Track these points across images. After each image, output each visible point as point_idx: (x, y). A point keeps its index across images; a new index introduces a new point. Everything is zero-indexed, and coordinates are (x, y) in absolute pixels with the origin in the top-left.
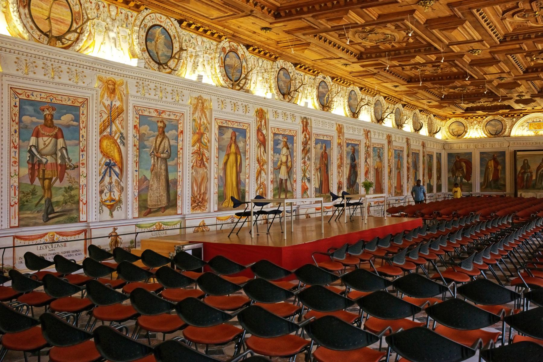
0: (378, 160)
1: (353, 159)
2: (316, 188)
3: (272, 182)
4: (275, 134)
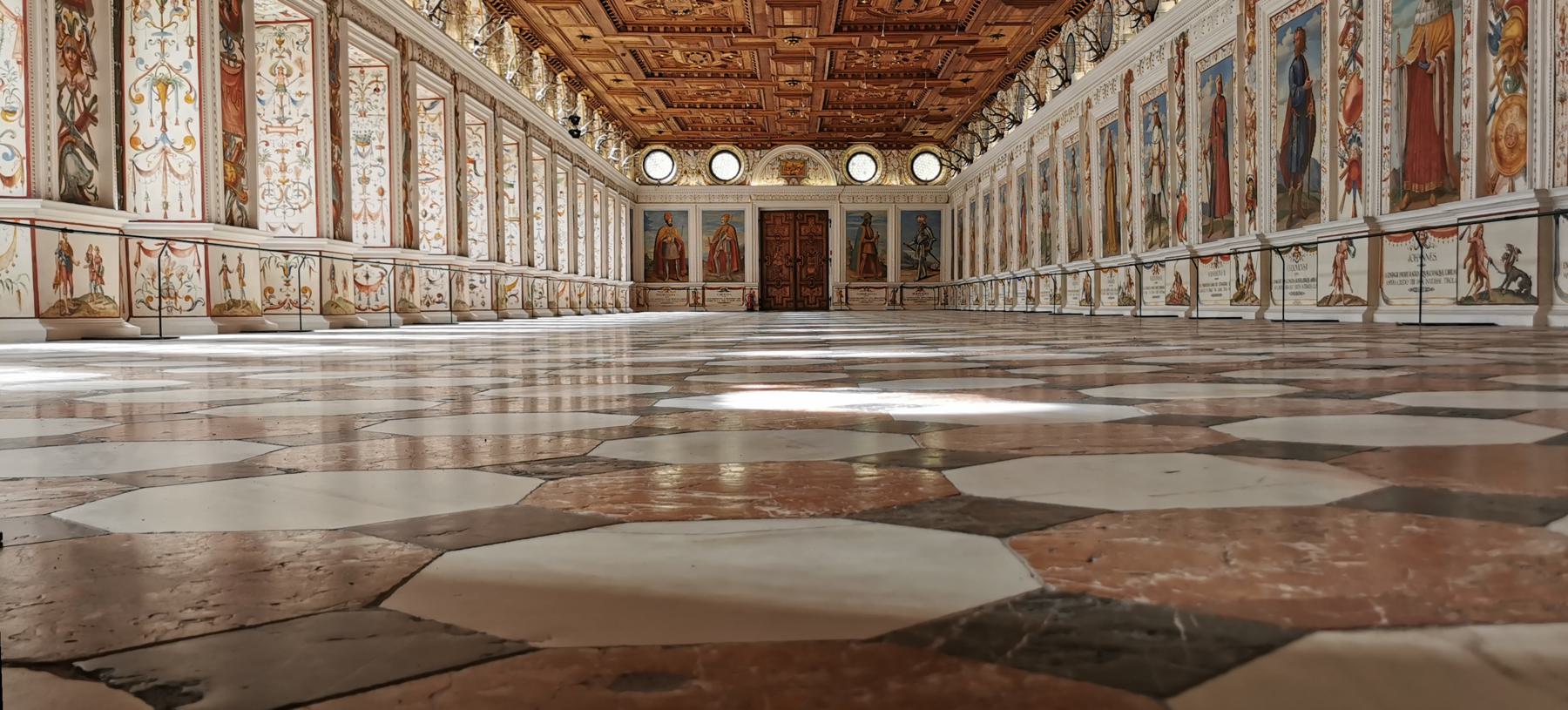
1: (1300, 75)
2: (1203, 203)
3: (1142, 202)
4: (1145, 106)
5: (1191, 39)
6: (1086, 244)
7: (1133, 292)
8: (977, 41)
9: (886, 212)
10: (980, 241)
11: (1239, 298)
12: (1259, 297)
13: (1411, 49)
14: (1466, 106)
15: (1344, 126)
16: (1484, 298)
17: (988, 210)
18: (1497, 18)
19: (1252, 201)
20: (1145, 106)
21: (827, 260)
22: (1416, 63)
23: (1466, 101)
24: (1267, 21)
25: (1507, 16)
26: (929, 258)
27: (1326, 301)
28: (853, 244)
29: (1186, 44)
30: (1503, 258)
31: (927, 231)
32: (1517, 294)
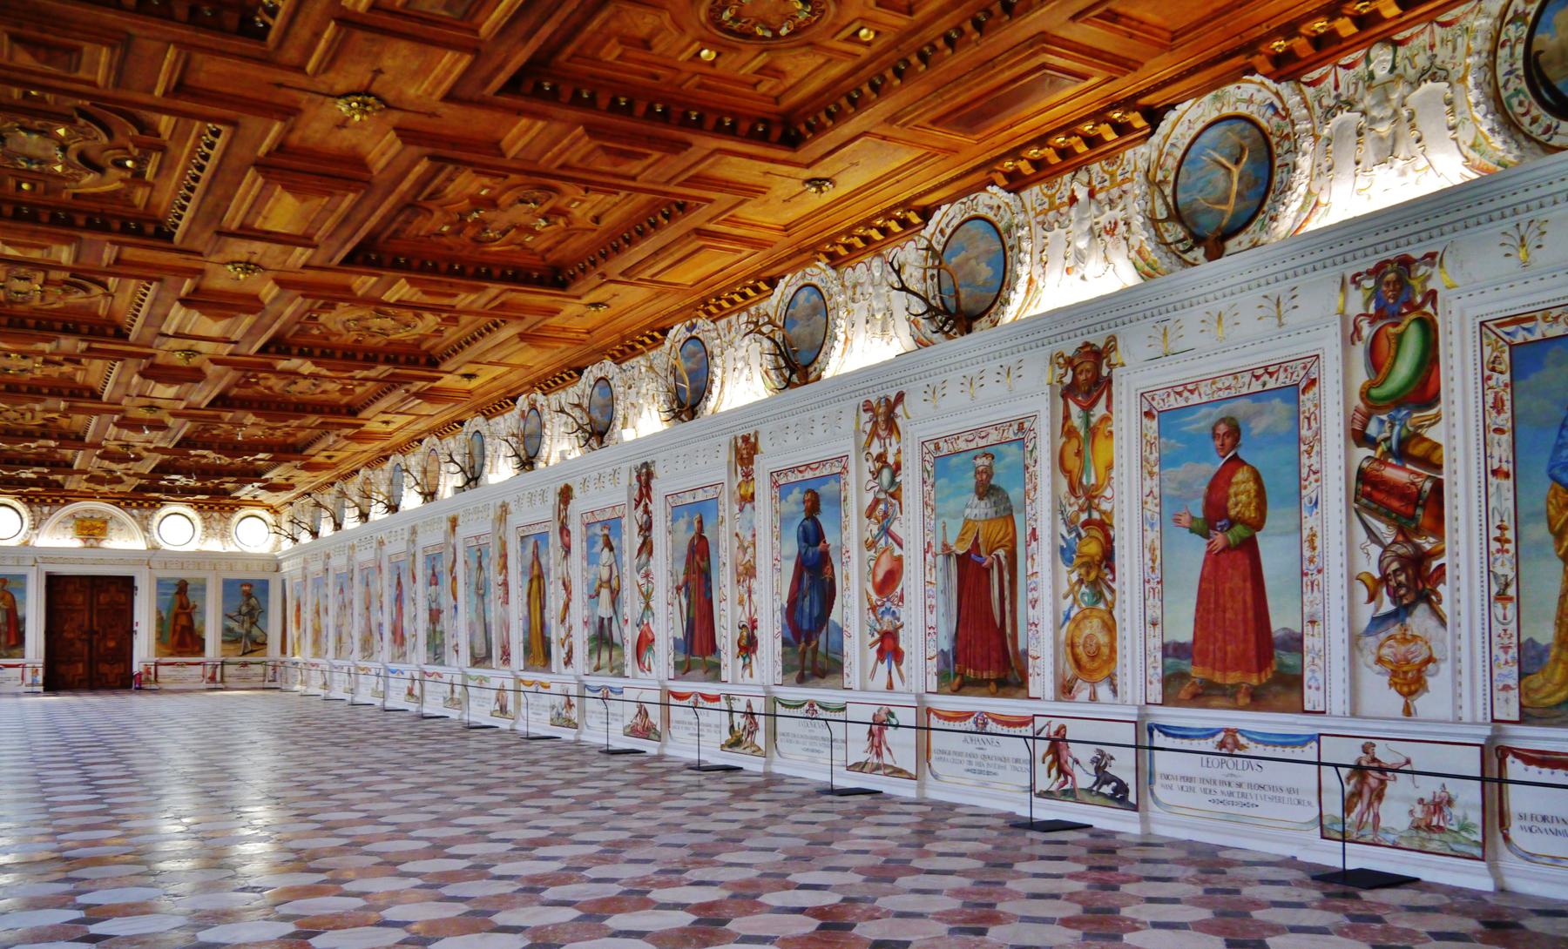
0: (980, 510)
1: (812, 535)
2: (675, 639)
3: (585, 623)
4: (588, 525)
5: (658, 470)
6: (496, 652)
7: (574, 714)
8: (363, 425)
9: (205, 579)
10: (330, 621)
11: (735, 743)
12: (763, 748)
13: (961, 539)
14: (1033, 607)
15: (874, 597)
16: (1070, 794)
17: (342, 591)
18: (1070, 532)
19: (748, 646)
20: (588, 525)
21: (129, 632)
22: (969, 552)
23: (1034, 603)
24: (767, 476)
25: (1083, 534)
26: (255, 631)
27: (860, 767)
28: (164, 614)
29: (650, 475)
30: (1092, 762)
31: (253, 601)
32: (1111, 797)
